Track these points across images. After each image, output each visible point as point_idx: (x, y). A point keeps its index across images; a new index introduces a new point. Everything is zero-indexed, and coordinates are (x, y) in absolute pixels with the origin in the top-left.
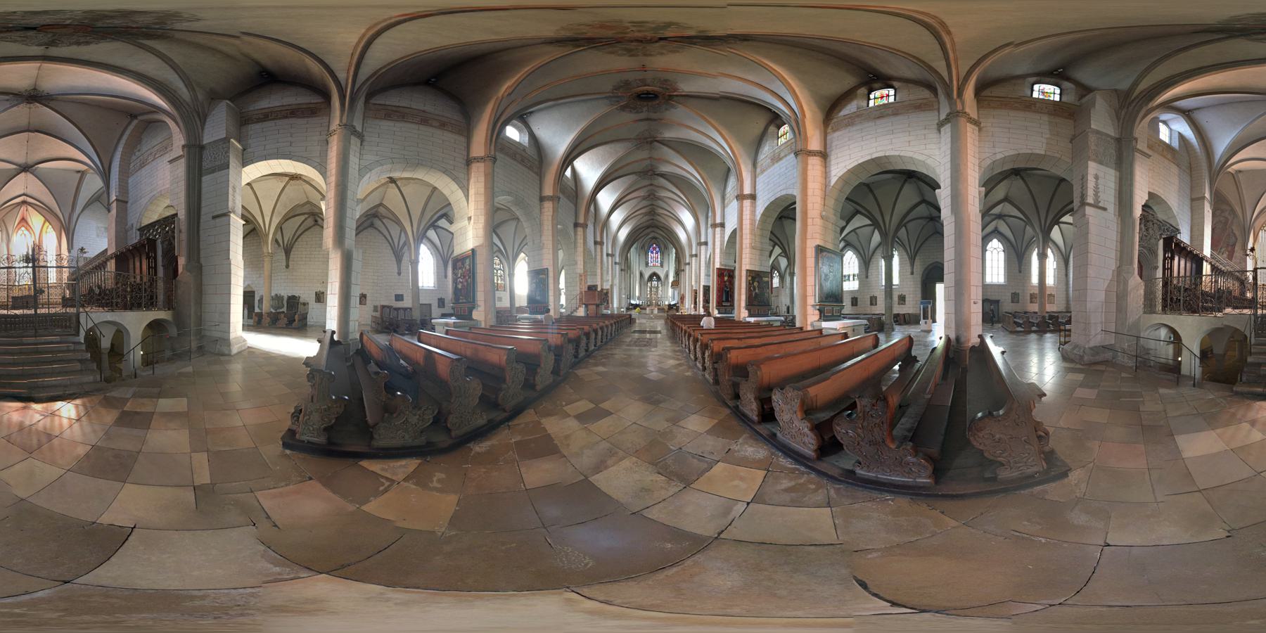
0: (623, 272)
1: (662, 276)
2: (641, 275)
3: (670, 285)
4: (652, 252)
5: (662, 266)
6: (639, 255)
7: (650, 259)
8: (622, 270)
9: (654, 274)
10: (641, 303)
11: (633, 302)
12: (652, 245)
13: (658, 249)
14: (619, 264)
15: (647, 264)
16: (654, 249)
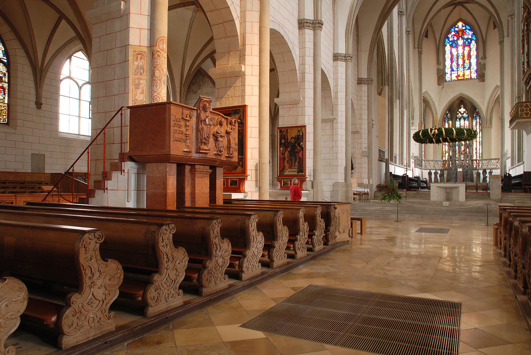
0: (365, 88)
1: (483, 106)
2: (426, 103)
3: (507, 118)
4: (454, 45)
5: (481, 76)
6: (420, 53)
7: (448, 63)
8: (360, 81)
9: (462, 101)
10: (426, 176)
11: (399, 171)
12: (454, 25)
13: (469, 34)
14: (346, 58)
15: (441, 77)
16: (460, 34)
